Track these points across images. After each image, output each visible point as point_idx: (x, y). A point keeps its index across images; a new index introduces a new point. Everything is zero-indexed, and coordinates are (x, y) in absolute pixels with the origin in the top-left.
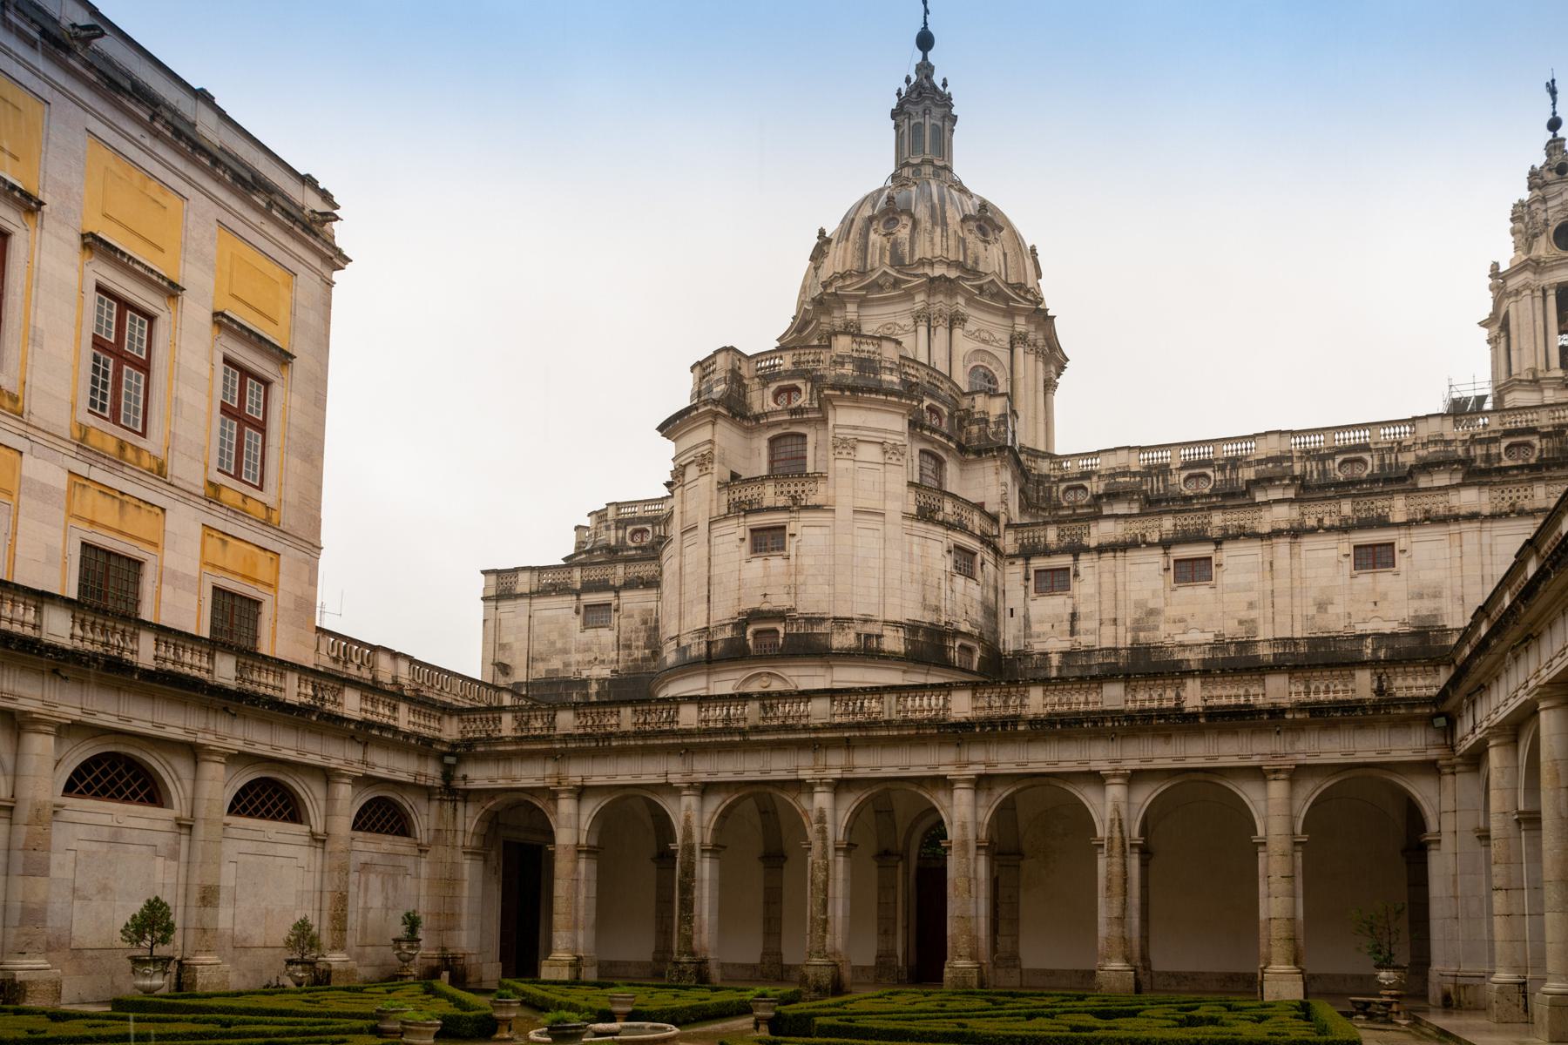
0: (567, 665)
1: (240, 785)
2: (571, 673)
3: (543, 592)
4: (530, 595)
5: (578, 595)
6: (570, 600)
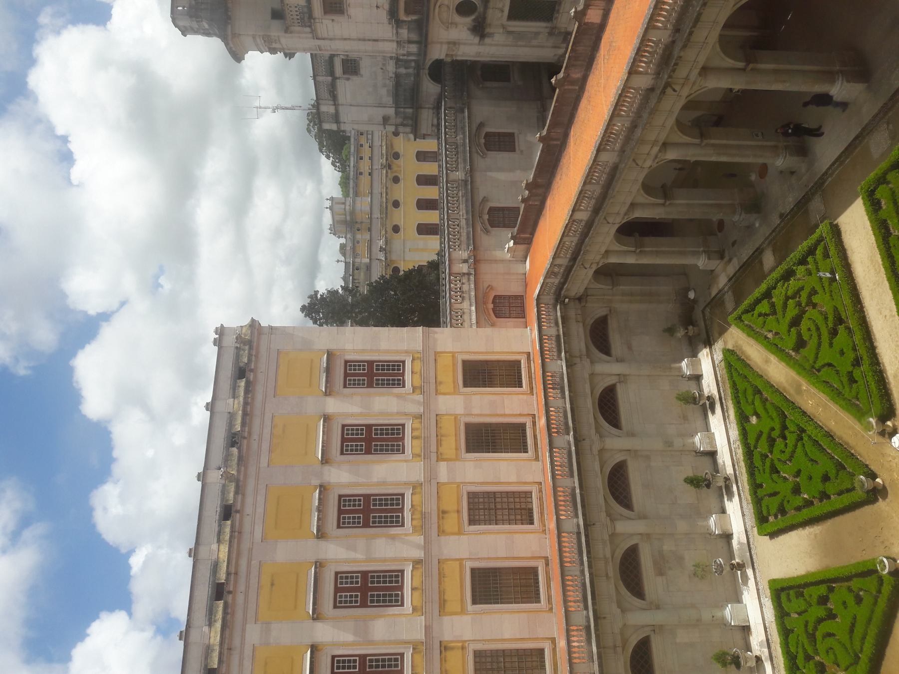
0: (385, 86)
1: (607, 424)
2: (390, 84)
3: (334, 97)
4: (336, 105)
5: (337, 78)
6: (340, 84)
